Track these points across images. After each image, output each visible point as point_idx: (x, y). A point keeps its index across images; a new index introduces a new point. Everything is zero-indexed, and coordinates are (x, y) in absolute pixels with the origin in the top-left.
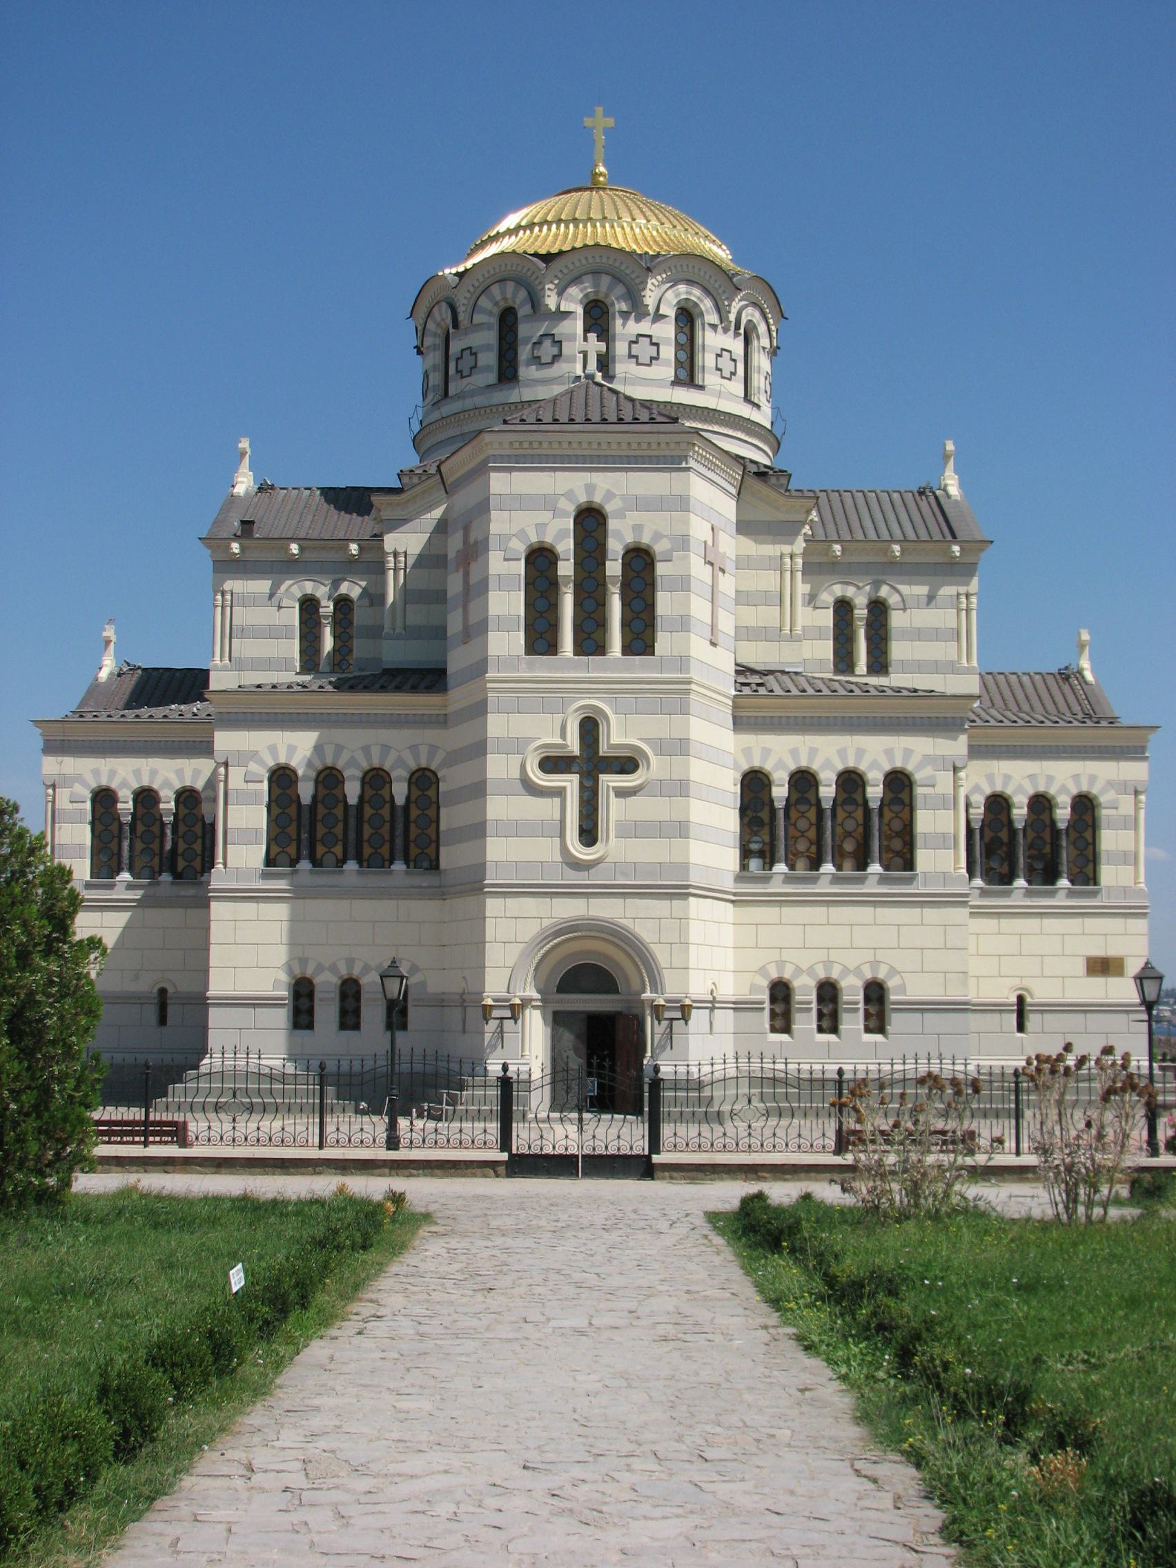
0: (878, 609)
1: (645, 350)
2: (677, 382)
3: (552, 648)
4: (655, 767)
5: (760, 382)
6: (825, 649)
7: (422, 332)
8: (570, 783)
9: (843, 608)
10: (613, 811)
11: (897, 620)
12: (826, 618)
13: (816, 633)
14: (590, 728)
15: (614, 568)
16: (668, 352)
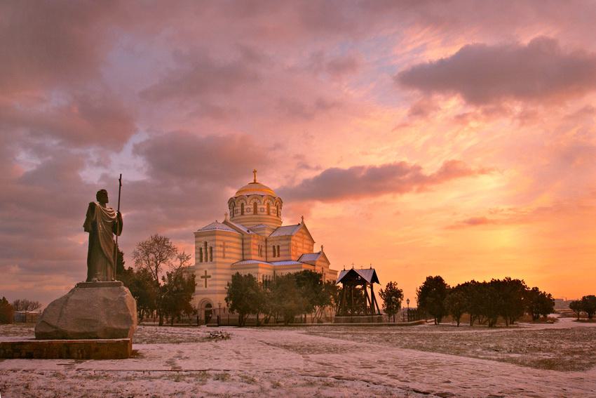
0: (278, 247)
1: (248, 210)
2: (254, 214)
3: (201, 261)
4: (213, 277)
5: (271, 211)
6: (272, 254)
7: (229, 206)
8: (204, 279)
9: (274, 247)
10: (208, 283)
11: (281, 248)
12: (272, 249)
13: (269, 251)
14: (206, 272)
15: (208, 250)
16: (252, 210)
